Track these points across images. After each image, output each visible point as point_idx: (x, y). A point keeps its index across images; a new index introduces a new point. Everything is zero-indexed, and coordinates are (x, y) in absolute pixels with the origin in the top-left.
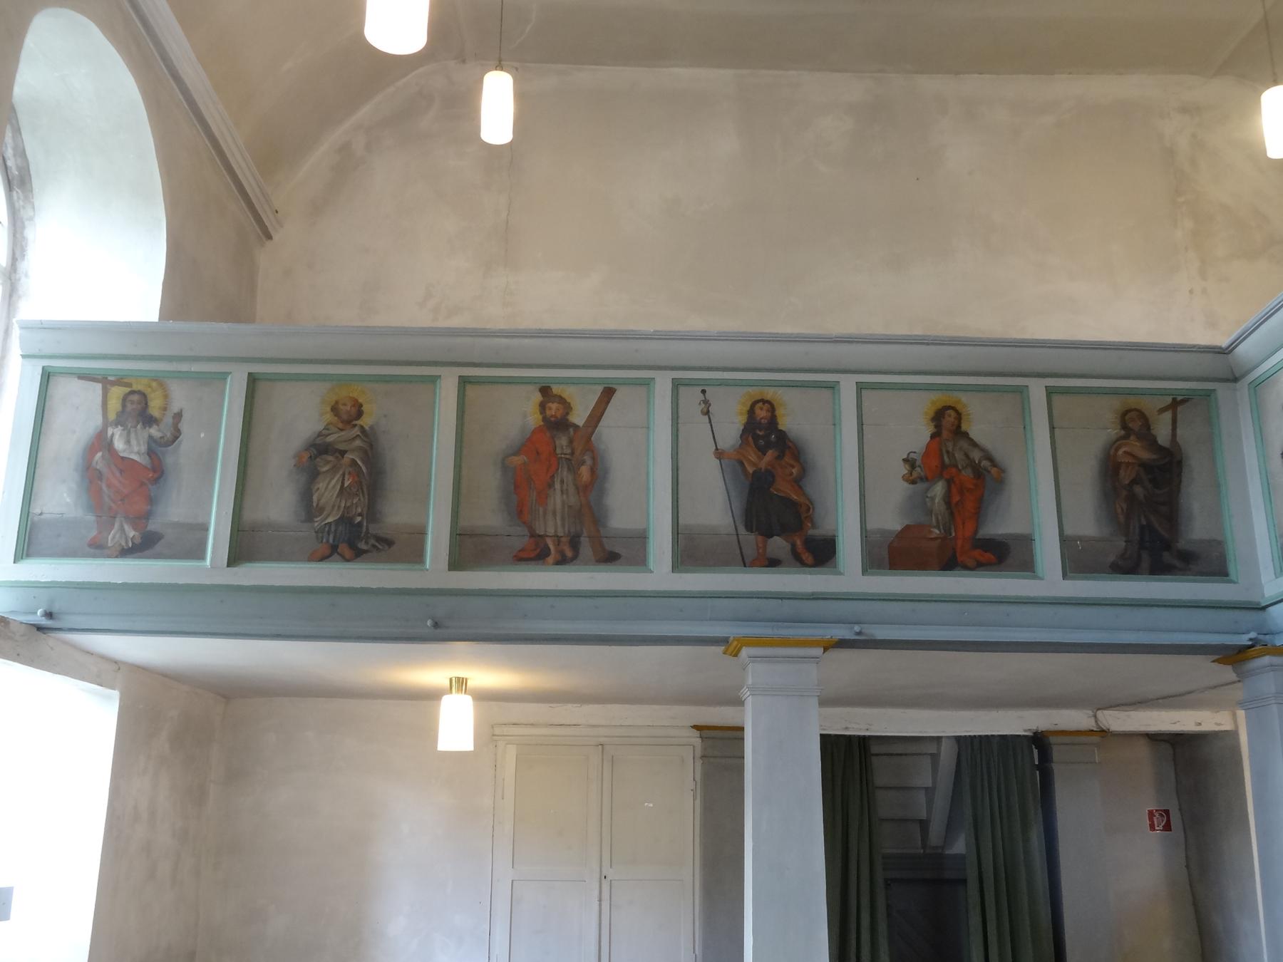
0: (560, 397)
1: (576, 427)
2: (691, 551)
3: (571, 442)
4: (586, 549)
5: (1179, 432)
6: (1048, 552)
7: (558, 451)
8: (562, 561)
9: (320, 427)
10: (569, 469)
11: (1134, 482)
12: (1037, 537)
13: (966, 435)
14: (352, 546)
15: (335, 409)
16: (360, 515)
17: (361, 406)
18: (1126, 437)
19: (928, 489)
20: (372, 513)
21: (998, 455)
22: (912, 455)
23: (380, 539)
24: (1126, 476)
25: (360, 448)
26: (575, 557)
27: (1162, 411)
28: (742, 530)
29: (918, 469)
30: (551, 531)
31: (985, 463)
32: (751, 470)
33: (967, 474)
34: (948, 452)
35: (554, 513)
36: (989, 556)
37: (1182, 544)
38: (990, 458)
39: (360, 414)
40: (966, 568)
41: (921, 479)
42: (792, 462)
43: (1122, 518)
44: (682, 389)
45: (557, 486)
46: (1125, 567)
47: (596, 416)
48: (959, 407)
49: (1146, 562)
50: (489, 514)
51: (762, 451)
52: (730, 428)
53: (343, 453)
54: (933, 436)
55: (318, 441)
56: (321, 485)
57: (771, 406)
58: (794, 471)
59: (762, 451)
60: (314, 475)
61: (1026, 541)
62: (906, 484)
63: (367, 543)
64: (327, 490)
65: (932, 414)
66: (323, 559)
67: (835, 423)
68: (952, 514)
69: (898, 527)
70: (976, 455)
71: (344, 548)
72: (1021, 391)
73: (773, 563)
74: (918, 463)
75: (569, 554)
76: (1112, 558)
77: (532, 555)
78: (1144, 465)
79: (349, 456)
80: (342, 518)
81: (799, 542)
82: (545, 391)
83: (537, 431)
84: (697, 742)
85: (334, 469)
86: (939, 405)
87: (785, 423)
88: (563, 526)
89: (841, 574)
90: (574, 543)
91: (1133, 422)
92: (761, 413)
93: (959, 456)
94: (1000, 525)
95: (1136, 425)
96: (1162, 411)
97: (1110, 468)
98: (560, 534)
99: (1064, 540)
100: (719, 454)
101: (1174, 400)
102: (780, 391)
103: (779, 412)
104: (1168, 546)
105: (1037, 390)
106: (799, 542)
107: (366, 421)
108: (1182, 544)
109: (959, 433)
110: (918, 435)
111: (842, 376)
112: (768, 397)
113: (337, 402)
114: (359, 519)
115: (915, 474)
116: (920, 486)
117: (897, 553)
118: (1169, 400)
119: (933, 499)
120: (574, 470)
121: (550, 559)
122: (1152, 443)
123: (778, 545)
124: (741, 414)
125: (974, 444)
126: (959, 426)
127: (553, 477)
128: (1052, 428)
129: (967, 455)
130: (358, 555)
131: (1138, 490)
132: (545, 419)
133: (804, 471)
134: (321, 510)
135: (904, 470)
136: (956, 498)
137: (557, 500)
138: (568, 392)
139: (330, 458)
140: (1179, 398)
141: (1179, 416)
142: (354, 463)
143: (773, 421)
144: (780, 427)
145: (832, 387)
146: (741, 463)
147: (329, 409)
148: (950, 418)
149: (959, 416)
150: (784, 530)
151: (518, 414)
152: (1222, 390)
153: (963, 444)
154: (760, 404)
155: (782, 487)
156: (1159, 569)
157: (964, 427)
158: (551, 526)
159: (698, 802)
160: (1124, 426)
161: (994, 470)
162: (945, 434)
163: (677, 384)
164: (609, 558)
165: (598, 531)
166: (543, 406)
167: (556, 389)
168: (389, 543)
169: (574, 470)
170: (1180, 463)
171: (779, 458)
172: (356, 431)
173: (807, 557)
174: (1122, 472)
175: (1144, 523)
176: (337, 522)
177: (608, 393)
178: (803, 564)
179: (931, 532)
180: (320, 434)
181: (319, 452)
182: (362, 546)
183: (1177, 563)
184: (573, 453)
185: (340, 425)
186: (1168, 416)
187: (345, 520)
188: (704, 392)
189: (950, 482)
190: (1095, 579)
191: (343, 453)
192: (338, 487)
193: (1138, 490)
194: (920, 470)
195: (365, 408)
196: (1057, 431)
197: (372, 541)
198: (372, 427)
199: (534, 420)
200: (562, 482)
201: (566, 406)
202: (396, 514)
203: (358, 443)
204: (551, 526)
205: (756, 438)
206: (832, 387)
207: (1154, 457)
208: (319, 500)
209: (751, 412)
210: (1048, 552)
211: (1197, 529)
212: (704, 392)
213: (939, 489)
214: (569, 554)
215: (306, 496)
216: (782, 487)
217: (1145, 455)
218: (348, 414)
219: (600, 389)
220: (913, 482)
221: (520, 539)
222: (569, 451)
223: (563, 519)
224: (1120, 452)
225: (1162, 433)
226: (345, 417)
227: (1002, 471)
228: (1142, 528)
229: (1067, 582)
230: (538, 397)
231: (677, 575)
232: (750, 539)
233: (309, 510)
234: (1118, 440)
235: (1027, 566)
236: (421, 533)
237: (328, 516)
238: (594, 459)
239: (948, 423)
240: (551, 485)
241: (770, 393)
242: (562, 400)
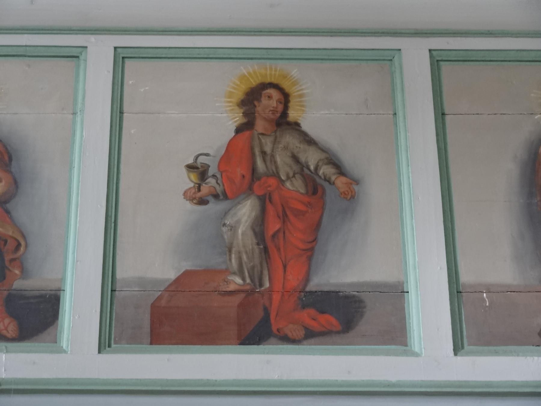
6: (429, 311)
12: (411, 287)
13: (296, 126)
19: (226, 213)
22: (202, 160)
31: (326, 170)
33: (296, 186)
34: (264, 153)
36: (330, 320)
40: (286, 339)
41: (216, 196)
48: (285, 85)
54: (239, 130)
61: (395, 293)
62: (189, 206)
65: (239, 95)
68: (266, 250)
69: (172, 275)
70: (312, 158)
86: (254, 82)
89: (61, 351)
93: (282, 160)
94: (343, 270)
99: (456, 291)
105: (415, 60)
109: (283, 122)
111: (92, 38)
115: (205, 189)
116: (214, 208)
119: (233, 229)
125: (309, 141)
126: (285, 114)
128: (440, 115)
129: (295, 159)
135: (187, 182)
136: (274, 226)
145: (74, 56)
148: (270, 102)
149: (286, 97)
153: (290, 140)
157: (293, 115)
161: (341, 181)
162: (260, 126)
179: (227, 282)
189: (264, 201)
194: (211, 183)
196: (448, 118)
210: (429, 311)
213: (246, 211)
220: (202, 202)
229: (459, 358)
235: (395, 335)
239: (266, 108)
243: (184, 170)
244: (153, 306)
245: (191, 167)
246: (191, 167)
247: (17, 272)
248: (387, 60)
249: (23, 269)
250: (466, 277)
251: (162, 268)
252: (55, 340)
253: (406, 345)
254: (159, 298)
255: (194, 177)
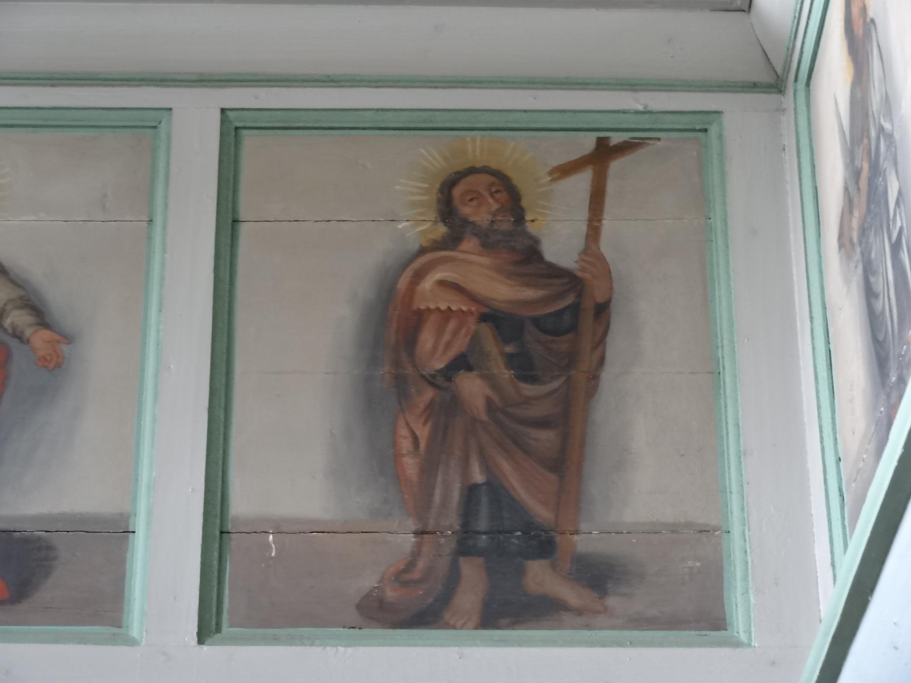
5: (607, 224)
6: (164, 565)
11: (462, 363)
12: (140, 525)
18: (452, 241)
24: (434, 349)
27: (565, 170)
31: (18, 318)
37: (588, 541)
43: (411, 465)
49: (471, 594)
76: (368, 581)
78: (492, 317)
91: (477, 202)
95: (480, 214)
96: (565, 170)
97: (393, 325)
99: (218, 529)
101: (602, 143)
104: (543, 544)
105: (195, 127)
108: (588, 541)
118: (588, 143)
122: (528, 258)
128: (229, 224)
131: (472, 388)
140: (616, 138)
141: (612, 186)
152: (739, 116)
160: (447, 209)
161: (40, 338)
170: (602, 310)
174: (426, 338)
175: (478, 477)
183: (569, 594)
186: (582, 181)
190: (290, 641)
193: (472, 388)
196: (244, 229)
207: (530, 294)
211: (635, 488)
217: (502, 291)
224: (427, 284)
225: (559, 236)
228: (471, 492)
229: (205, 648)
234: (422, 251)
248: (148, 127)
250: (242, 504)
253: (119, 625)
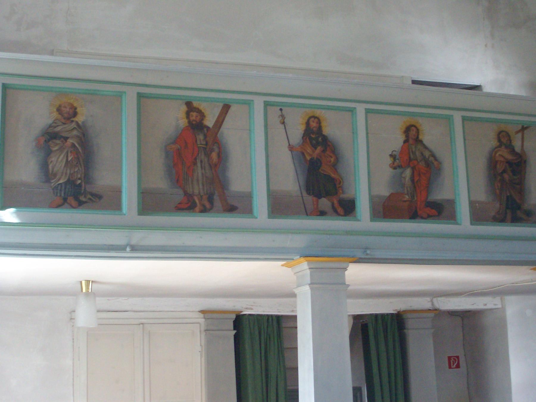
0: (198, 109)
1: (208, 128)
2: (279, 206)
3: (205, 137)
4: (217, 203)
5: (525, 144)
6: (463, 210)
7: (198, 142)
8: (204, 210)
9: (50, 121)
10: (205, 154)
11: (504, 171)
13: (421, 141)
14: (76, 198)
15: (59, 110)
16: (79, 179)
17: (76, 109)
18: (500, 146)
19: (402, 173)
20: (87, 178)
21: (438, 153)
22: (394, 153)
23: (92, 194)
24: (500, 168)
25: (77, 137)
26: (211, 208)
27: (517, 132)
28: (305, 194)
29: (397, 161)
30: (196, 191)
31: (431, 159)
32: (308, 158)
33: (422, 164)
34: (412, 152)
35: (198, 180)
36: (434, 212)
37: (526, 207)
38: (433, 155)
39: (75, 114)
40: (422, 218)
42: (331, 155)
43: (498, 191)
44: (268, 107)
45: (199, 164)
46: (499, 219)
47: (219, 122)
48: (417, 125)
49: (509, 216)
50: (159, 181)
51: (315, 147)
52: (297, 132)
53: (66, 139)
54: (405, 142)
55: (50, 130)
56: (54, 159)
57: (318, 120)
58: (332, 160)
59: (315, 147)
60: (48, 153)
61: (452, 203)
62: (391, 170)
63: (85, 197)
64: (58, 162)
65: (404, 129)
66: (59, 206)
67: (354, 132)
68: (415, 187)
70: (427, 154)
71: (71, 199)
72: (449, 119)
73: (322, 214)
74: (397, 157)
75: (208, 206)
76: (493, 214)
77: (186, 206)
78: (509, 163)
79: (70, 141)
80: (69, 180)
81: (335, 202)
82: (189, 104)
83: (184, 130)
84: (202, 321)
85: (61, 149)
86: (408, 124)
87: (327, 131)
88: (204, 190)
90: (210, 199)
91: (503, 138)
92: (314, 124)
93: (418, 153)
94: (439, 195)
95: (504, 140)
96: (517, 132)
98: (202, 194)
99: (472, 204)
100: (291, 148)
101: (523, 126)
102: (323, 111)
103: (323, 124)
104: (519, 208)
106: (335, 202)
107: (80, 119)
108: (526, 207)
109: (418, 141)
110: (397, 141)
111: (357, 104)
112: (317, 115)
113: (60, 106)
114: (79, 182)
116: (399, 171)
117: (386, 209)
118: (520, 127)
119: (404, 178)
120: (208, 155)
121: (197, 209)
122: (512, 151)
123: (325, 203)
124: (302, 124)
125: (426, 148)
126: (418, 137)
127: (195, 159)
129: (422, 154)
130: (80, 204)
131: (506, 176)
132: (189, 122)
133: (337, 159)
134: (55, 175)
135: (390, 161)
136: (416, 179)
137: (199, 171)
138: (203, 106)
139: (58, 142)
140: (525, 126)
141: (525, 136)
142: (73, 145)
143: (320, 128)
144: (323, 133)
145: (352, 111)
146: (303, 154)
147: (55, 110)
148: (413, 132)
149: (418, 130)
150: (328, 194)
151: (174, 119)
153: (420, 147)
154: (313, 119)
155: (326, 169)
156: (515, 220)
157: (420, 137)
158: (197, 189)
159: (203, 359)
160: (499, 140)
162: (411, 141)
163: (267, 104)
164: (231, 209)
165: (224, 193)
166: (188, 114)
167: (195, 104)
168: (99, 197)
169: (208, 155)
170: (525, 162)
171: (324, 151)
172: (74, 125)
173: (340, 210)
174: (498, 166)
175: (508, 194)
176: (65, 183)
177: (226, 108)
178: (338, 214)
179: (405, 197)
180: (50, 126)
181: (50, 137)
182: (82, 199)
183: (523, 216)
184: (207, 144)
185: (64, 121)
186: (520, 135)
187: (70, 182)
188: (281, 110)
189: (413, 169)
191: (66, 139)
192: (65, 160)
193: (506, 176)
195: (78, 110)
197: (89, 196)
198: (83, 122)
199: (183, 122)
200: (201, 162)
201: (202, 115)
202: (102, 179)
203: (75, 133)
204: (197, 189)
205: (311, 139)
206: (352, 111)
207: (515, 158)
208: (53, 169)
209: (308, 123)
210: (463, 210)
212: (281, 110)
213: (408, 173)
214: (208, 206)
215: (44, 166)
216: (326, 169)
217: (510, 157)
218: (68, 113)
219: (221, 105)
220: (395, 168)
221: (178, 196)
222: (204, 143)
223: (203, 185)
224: (497, 155)
225: (517, 145)
226: (66, 115)
227: (440, 163)
228: (508, 197)
230: (184, 108)
231: (271, 220)
232: (309, 199)
233: (47, 174)
234: (496, 148)
235: (452, 217)
236: (118, 192)
237: (59, 180)
238: (219, 148)
239: (412, 134)
240: (195, 164)
241: (318, 113)
242: (199, 111)
243: (389, 157)
244: (383, 205)
245: (391, 156)
246: (391, 156)
247: (341, 191)
249: (342, 190)
251: (384, 191)
252: (355, 216)
254: (384, 203)
255: (392, 159)
